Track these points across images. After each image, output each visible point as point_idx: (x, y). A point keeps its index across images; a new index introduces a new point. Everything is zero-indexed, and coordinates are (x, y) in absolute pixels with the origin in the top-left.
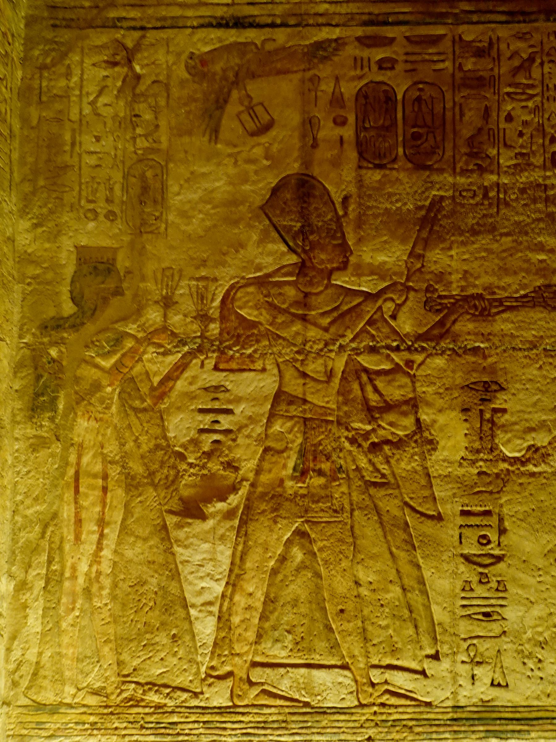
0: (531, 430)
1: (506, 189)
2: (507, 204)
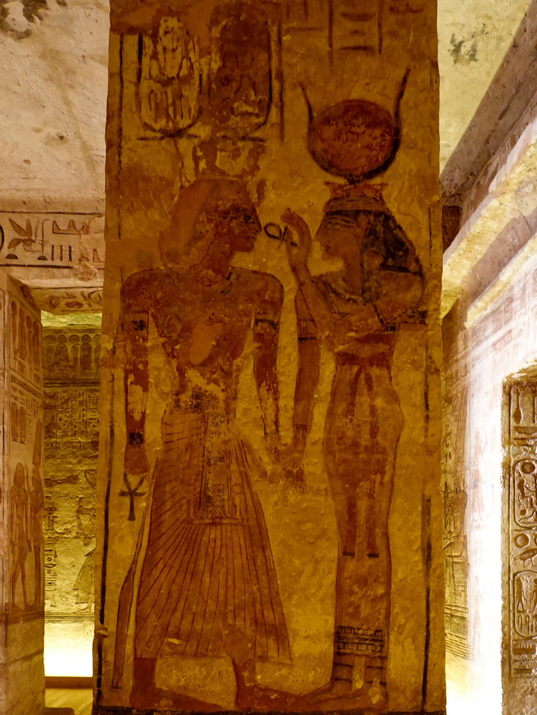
0: (65, 523)
2: (59, 448)
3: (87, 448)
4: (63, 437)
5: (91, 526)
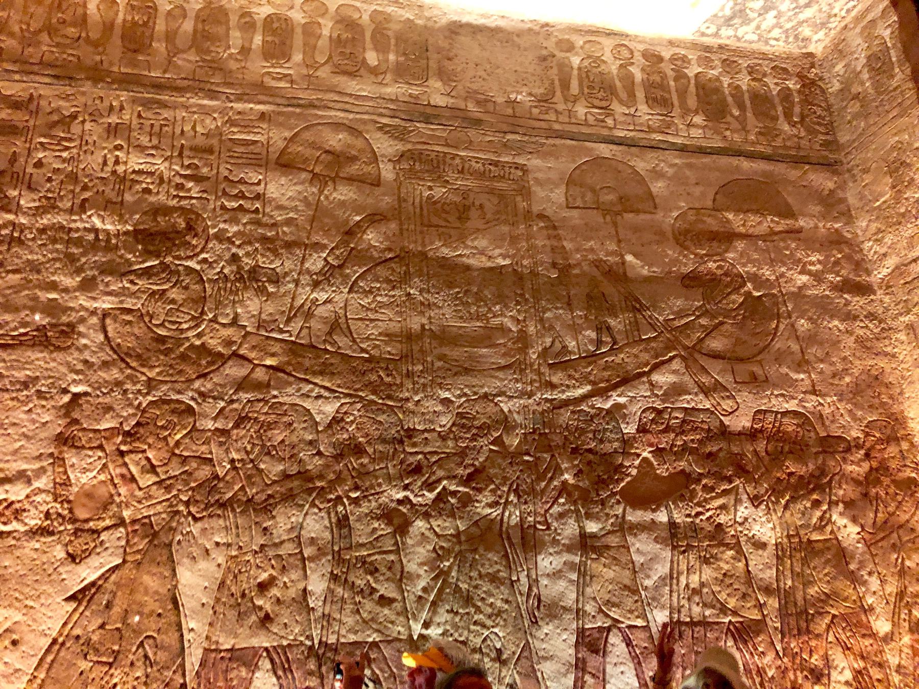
1: (22, 228)
3: (117, 247)
4: (39, 211)
5: (103, 491)
